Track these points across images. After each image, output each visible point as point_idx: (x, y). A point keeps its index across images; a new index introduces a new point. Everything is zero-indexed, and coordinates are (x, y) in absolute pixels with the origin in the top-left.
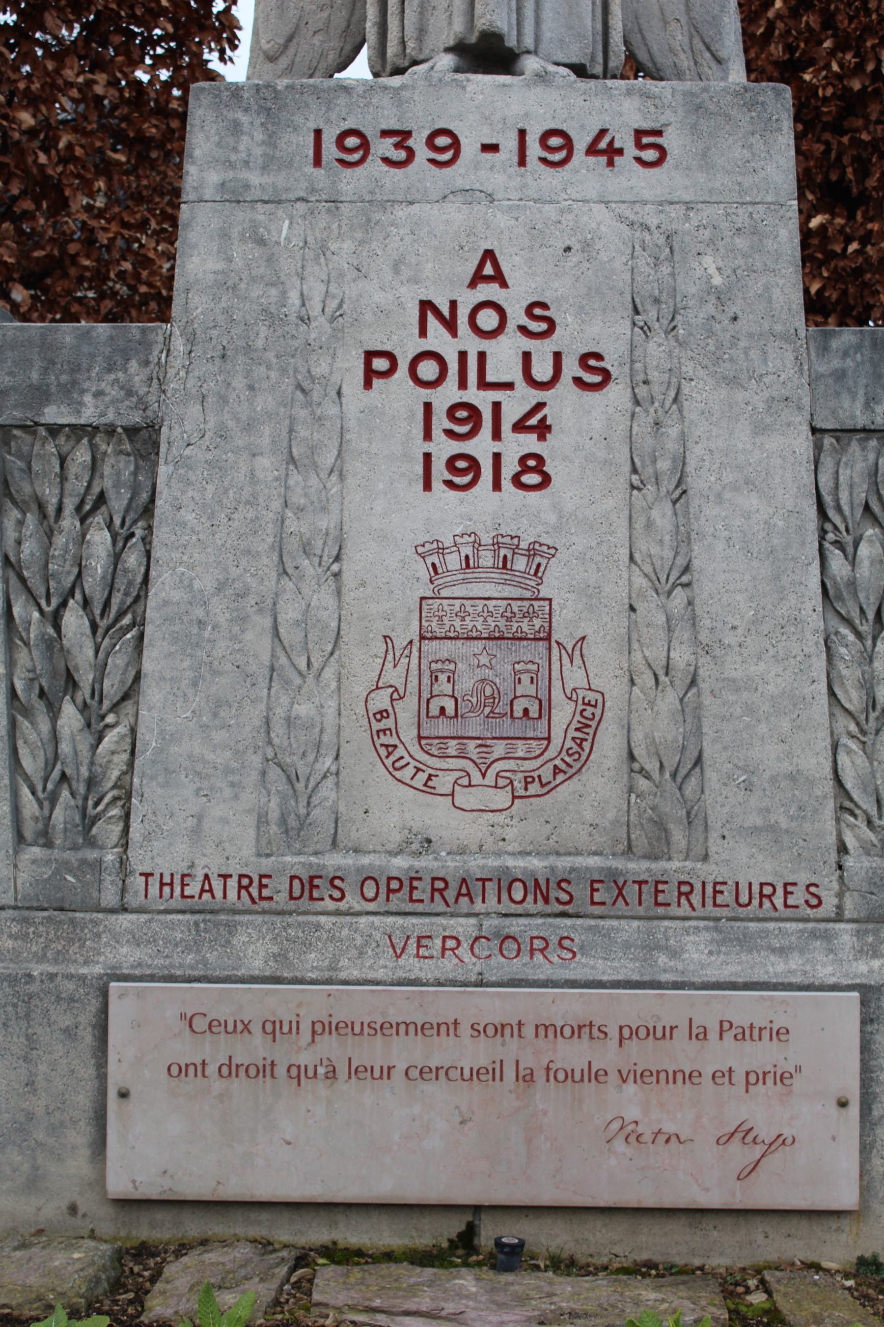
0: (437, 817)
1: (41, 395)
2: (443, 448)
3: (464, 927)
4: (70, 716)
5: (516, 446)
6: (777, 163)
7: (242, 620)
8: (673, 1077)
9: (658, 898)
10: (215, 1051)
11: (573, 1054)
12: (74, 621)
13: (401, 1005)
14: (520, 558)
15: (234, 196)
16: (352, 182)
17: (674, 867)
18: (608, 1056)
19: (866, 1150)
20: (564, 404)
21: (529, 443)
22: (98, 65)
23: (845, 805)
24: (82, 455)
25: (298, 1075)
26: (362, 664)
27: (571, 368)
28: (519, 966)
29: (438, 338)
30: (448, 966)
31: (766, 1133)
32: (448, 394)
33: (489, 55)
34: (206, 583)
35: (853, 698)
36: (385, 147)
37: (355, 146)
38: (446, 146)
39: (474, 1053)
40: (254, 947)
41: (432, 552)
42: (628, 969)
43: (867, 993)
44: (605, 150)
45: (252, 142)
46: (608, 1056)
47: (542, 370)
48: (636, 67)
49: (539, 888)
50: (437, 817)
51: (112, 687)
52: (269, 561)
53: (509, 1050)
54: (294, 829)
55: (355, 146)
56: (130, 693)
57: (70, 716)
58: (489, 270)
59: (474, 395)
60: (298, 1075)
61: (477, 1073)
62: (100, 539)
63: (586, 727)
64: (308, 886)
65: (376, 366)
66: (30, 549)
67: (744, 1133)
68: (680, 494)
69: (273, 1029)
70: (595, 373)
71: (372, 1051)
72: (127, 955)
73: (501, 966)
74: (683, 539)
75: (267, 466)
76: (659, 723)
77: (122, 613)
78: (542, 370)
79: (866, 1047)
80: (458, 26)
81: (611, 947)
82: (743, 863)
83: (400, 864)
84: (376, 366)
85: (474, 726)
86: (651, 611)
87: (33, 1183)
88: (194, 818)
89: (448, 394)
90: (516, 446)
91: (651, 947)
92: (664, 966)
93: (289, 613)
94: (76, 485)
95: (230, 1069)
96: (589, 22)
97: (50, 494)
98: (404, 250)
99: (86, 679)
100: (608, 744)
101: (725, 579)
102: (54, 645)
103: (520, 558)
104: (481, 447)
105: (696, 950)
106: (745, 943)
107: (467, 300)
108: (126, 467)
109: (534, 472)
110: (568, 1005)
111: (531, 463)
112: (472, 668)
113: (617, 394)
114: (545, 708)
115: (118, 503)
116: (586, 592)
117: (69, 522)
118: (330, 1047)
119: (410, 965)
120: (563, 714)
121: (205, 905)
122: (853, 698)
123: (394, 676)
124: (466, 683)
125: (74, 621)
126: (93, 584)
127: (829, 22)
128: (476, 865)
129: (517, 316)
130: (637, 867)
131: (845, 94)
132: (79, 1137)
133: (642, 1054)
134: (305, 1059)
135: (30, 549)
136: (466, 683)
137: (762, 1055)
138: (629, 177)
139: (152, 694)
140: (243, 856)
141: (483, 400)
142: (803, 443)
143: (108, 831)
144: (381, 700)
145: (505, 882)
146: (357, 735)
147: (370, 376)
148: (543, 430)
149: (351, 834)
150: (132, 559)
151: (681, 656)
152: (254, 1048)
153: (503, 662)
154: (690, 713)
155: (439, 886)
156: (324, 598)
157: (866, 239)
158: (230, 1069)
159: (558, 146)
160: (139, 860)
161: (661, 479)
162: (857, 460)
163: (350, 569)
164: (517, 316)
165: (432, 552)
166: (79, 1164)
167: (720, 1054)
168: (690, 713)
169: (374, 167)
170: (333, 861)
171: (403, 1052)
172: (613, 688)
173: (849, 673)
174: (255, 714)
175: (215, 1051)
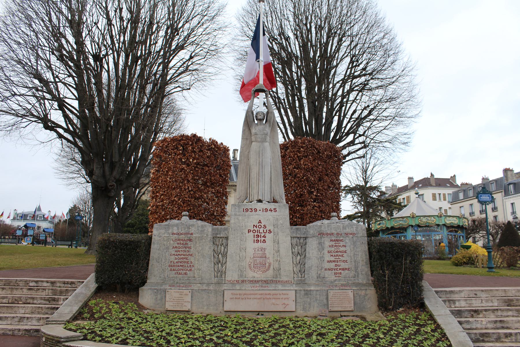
0: (255, 275)
1: (217, 234)
2: (256, 239)
3: (258, 285)
4: (220, 265)
5: (263, 239)
6: (287, 211)
7: (236, 256)
8: (278, 298)
9: (276, 282)
10: (235, 297)
11: (268, 296)
12: (220, 256)
13: (252, 292)
14: (263, 249)
15: (235, 215)
16: (247, 213)
17: (278, 279)
18: (271, 297)
19: (296, 306)
20: (267, 235)
21: (264, 238)
22: (213, 188)
23: (294, 273)
24: (221, 240)
25: (242, 299)
26: (248, 260)
27: (268, 231)
28: (263, 289)
29: (255, 228)
30: (256, 289)
31: (286, 304)
32: (256, 234)
33: (260, 201)
34: (233, 252)
35: (295, 263)
36: (250, 210)
37: (247, 210)
38: (256, 210)
39: (259, 296)
40: (238, 287)
41: (254, 249)
42: (274, 289)
43: (296, 291)
44: (271, 210)
45: (237, 210)
46: (271, 297)
47: (265, 231)
48: (275, 201)
49: (265, 281)
50: (255, 275)
51: (224, 262)
52: (239, 250)
53: (262, 296)
54: (241, 276)
55: (247, 210)
56: (226, 263)
57: (220, 265)
58: (260, 222)
59: (258, 234)
60: (242, 299)
61: (259, 298)
62: (223, 248)
63: (269, 266)
64: (243, 281)
65: (249, 231)
66: (216, 249)
67: (284, 304)
68: (278, 243)
69: (240, 294)
70: (270, 232)
71: (249, 296)
72: (226, 288)
73: (261, 289)
74: (278, 247)
75: (239, 241)
76: (276, 265)
77: (225, 255)
78: (265, 231)
79: (296, 296)
80: (257, 199)
81: (272, 287)
82: (285, 279)
83: (252, 279)
84: (249, 231)
85: (259, 266)
86: (276, 254)
87: (217, 310)
88: (232, 275)
89: (256, 234)
90: (263, 239)
91: (276, 287)
92: (277, 288)
93: (241, 255)
94: (220, 243)
95: (236, 298)
96: (269, 197)
97: (218, 243)
98: (252, 220)
99: (221, 261)
100: (272, 267)
101: (283, 251)
102: (218, 258)
103: (263, 249)
104: (259, 239)
105: (280, 287)
106: (285, 286)
107: (258, 225)
108: (225, 241)
109: (264, 241)
110: (268, 292)
111: (264, 240)
112: (259, 260)
113: (272, 234)
114: (266, 264)
115: (224, 244)
116: (269, 253)
117: (220, 246)
118: (245, 296)
119: (253, 289)
120: (267, 265)
121: (233, 283)
122: (295, 263)
123: (251, 261)
124: (258, 262)
125: (220, 256)
126: (222, 252)
127: (299, 185)
128: (259, 279)
129: (263, 226)
130: (274, 279)
131: (301, 194)
132: (221, 305)
133: (275, 296)
134: (243, 297)
135: (216, 249)
136: (258, 262)
137: (286, 296)
138: (273, 213)
139: (228, 263)
140: (237, 279)
141: (259, 234)
142: (290, 238)
143: (223, 276)
144: (250, 263)
145: (262, 281)
146: (247, 267)
147: (249, 232)
148: (265, 237)
149: (247, 277)
150: (226, 250)
151: (278, 259)
152: (238, 296)
153: (261, 259)
154: (279, 264)
155: (255, 281)
156: (244, 253)
157: (303, 210)
158: (236, 298)
159: (266, 210)
160: (226, 279)
161: (276, 242)
162: (295, 240)
163: (247, 250)
164: (263, 226)
165: (254, 249)
166: (221, 308)
167: (282, 296)
168: (279, 264)
169: (249, 212)
170: (245, 279)
171: (252, 296)
172: (272, 262)
173: (294, 260)
174: (238, 265)
175: (235, 297)
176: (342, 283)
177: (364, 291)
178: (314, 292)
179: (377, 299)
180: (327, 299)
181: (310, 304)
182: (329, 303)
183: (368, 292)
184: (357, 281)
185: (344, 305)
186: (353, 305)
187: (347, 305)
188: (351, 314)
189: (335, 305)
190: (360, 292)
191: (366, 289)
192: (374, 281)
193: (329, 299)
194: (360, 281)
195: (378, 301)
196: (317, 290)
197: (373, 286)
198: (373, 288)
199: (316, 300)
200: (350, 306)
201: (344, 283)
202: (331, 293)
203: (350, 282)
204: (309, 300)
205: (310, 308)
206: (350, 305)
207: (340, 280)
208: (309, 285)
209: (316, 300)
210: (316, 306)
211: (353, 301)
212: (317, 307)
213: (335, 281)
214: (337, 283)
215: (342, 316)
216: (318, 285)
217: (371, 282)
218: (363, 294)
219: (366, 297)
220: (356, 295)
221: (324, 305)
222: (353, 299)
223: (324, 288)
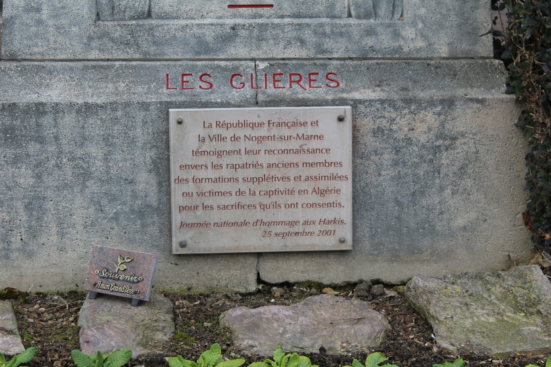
176: (278, 52)
177: (430, 118)
178: (68, 120)
179: (522, 169)
180: (162, 167)
181: (34, 204)
182: (177, 199)
183: (464, 120)
184: (385, 41)
185: (283, 215)
186: (345, 213)
187: (300, 215)
188: (336, 272)
189: (216, 216)
190: (402, 123)
191: (449, 103)
192: (515, 43)
193: (175, 172)
194: (412, 40)
195: (531, 184)
196: (88, 109)
197: (502, 79)
198: (498, 94)
199: (84, 175)
200: (322, 218)
201: (294, 52)
202: (189, 132)
203: (338, 48)
204: (25, 177)
205: (34, 233)
206: (330, 214)
207: (260, 34)
208: (35, 68)
209: (84, 175)
210: (78, 218)
211: (346, 188)
212: (90, 225)
213: (230, 36)
214: (242, 51)
215: (265, 291)
216: (101, 69)
217: (486, 46)
218: (421, 134)
219: (445, 158)
220: (369, 141)
221: (141, 214)
222: (347, 170)
223: (141, 93)
